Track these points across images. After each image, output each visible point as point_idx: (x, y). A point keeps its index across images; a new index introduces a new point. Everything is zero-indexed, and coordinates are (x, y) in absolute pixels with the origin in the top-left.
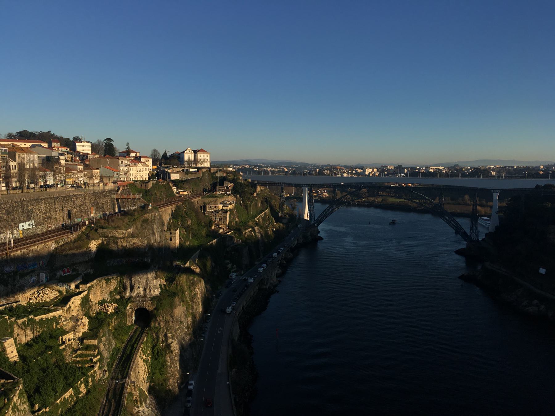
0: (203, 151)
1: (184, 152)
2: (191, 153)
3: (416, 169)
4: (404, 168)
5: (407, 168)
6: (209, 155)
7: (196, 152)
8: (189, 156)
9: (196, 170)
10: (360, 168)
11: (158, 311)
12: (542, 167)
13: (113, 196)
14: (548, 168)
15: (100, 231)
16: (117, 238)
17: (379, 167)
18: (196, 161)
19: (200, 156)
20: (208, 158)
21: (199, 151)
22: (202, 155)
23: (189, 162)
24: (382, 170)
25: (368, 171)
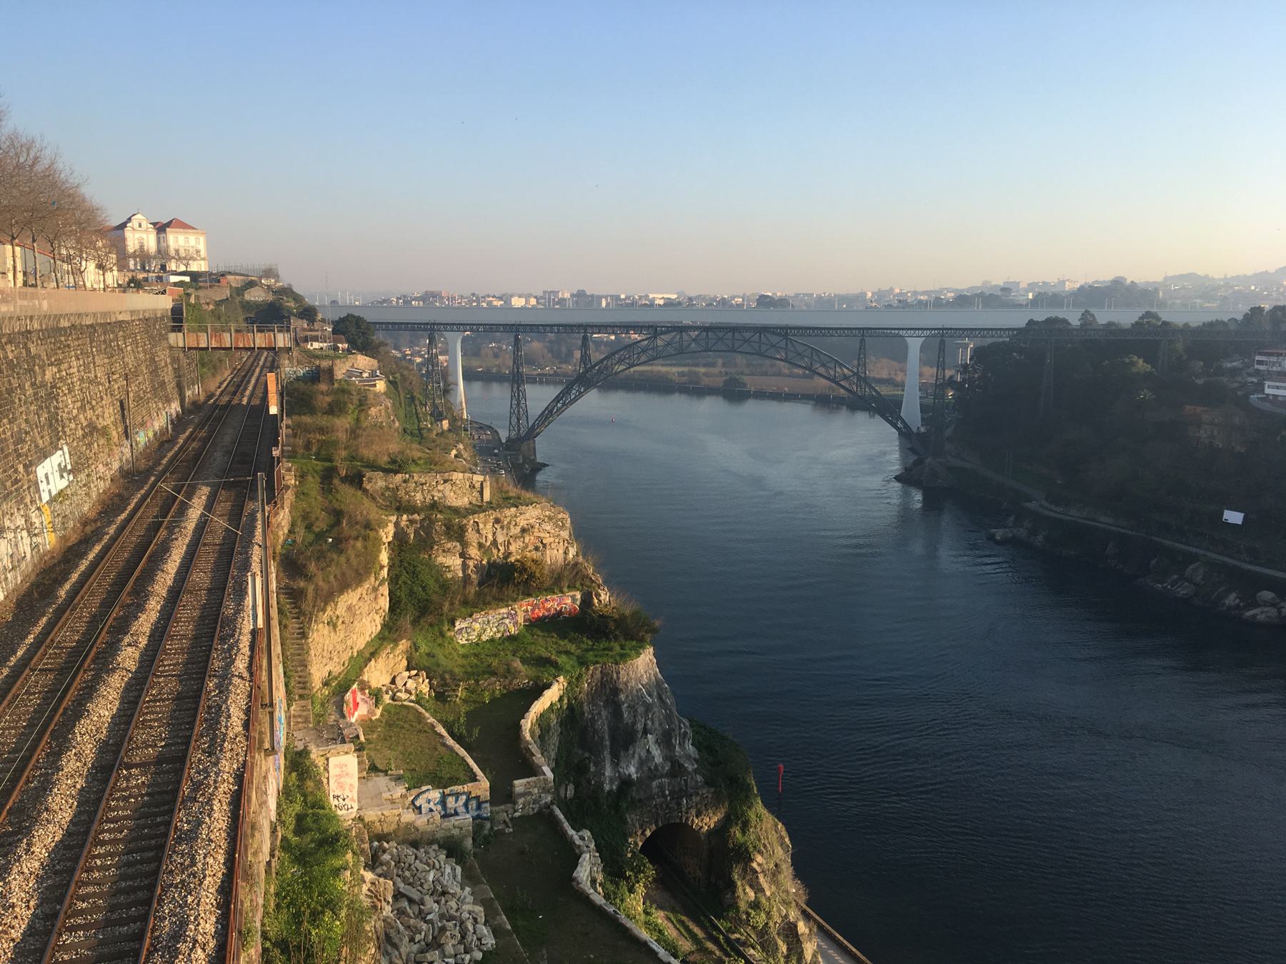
0: (184, 226)
1: (123, 226)
2: (146, 231)
3: (618, 298)
4: (600, 298)
5: (606, 297)
6: (202, 239)
7: (161, 228)
8: (140, 237)
9: (187, 279)
10: (500, 298)
11: (745, 827)
12: (870, 295)
13: (176, 339)
14: (880, 295)
15: (377, 482)
16: (456, 511)
17: (540, 294)
18: (163, 253)
19: (176, 240)
20: (202, 247)
21: (169, 224)
22: (181, 238)
23: (143, 256)
24: (549, 298)
25: (518, 302)
